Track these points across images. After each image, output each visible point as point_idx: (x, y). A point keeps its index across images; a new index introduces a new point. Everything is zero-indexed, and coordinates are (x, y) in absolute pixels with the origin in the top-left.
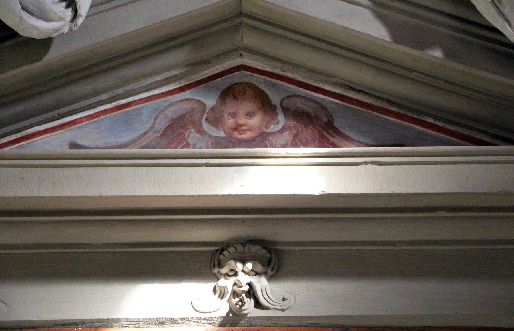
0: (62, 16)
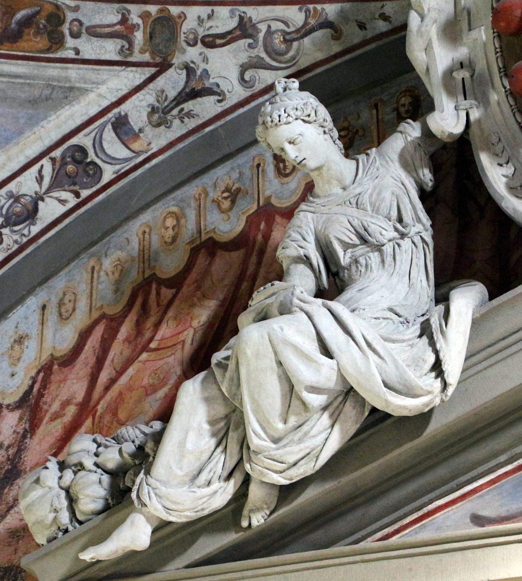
0: (429, 389)
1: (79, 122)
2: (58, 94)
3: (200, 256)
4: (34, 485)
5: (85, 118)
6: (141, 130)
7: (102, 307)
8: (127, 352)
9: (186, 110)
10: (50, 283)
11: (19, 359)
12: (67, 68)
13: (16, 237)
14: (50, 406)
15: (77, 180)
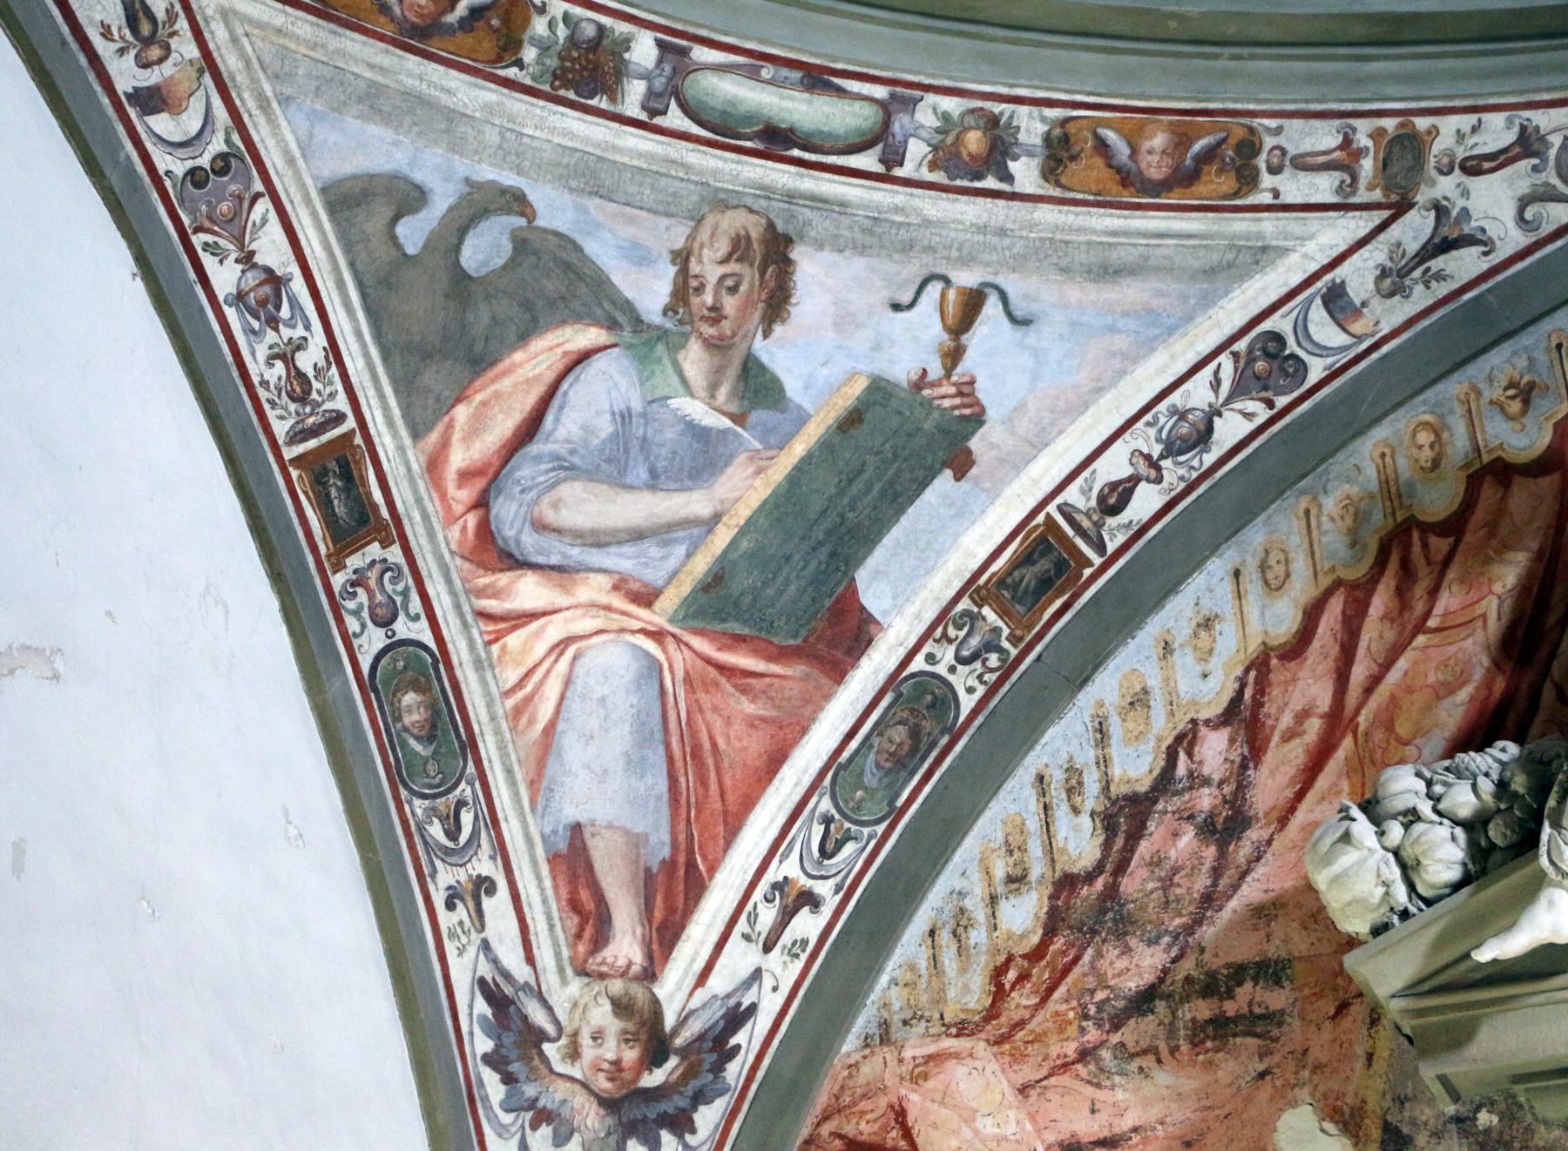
1: (1274, 297)
2: (1245, 258)
3: (1486, 486)
4: (1340, 845)
5: (1284, 291)
6: (1364, 304)
7: (1333, 569)
8: (1390, 635)
9: (1434, 270)
10: (1240, 536)
11: (1211, 651)
12: (1259, 220)
13: (1182, 471)
14: (1277, 719)
15: (1271, 382)
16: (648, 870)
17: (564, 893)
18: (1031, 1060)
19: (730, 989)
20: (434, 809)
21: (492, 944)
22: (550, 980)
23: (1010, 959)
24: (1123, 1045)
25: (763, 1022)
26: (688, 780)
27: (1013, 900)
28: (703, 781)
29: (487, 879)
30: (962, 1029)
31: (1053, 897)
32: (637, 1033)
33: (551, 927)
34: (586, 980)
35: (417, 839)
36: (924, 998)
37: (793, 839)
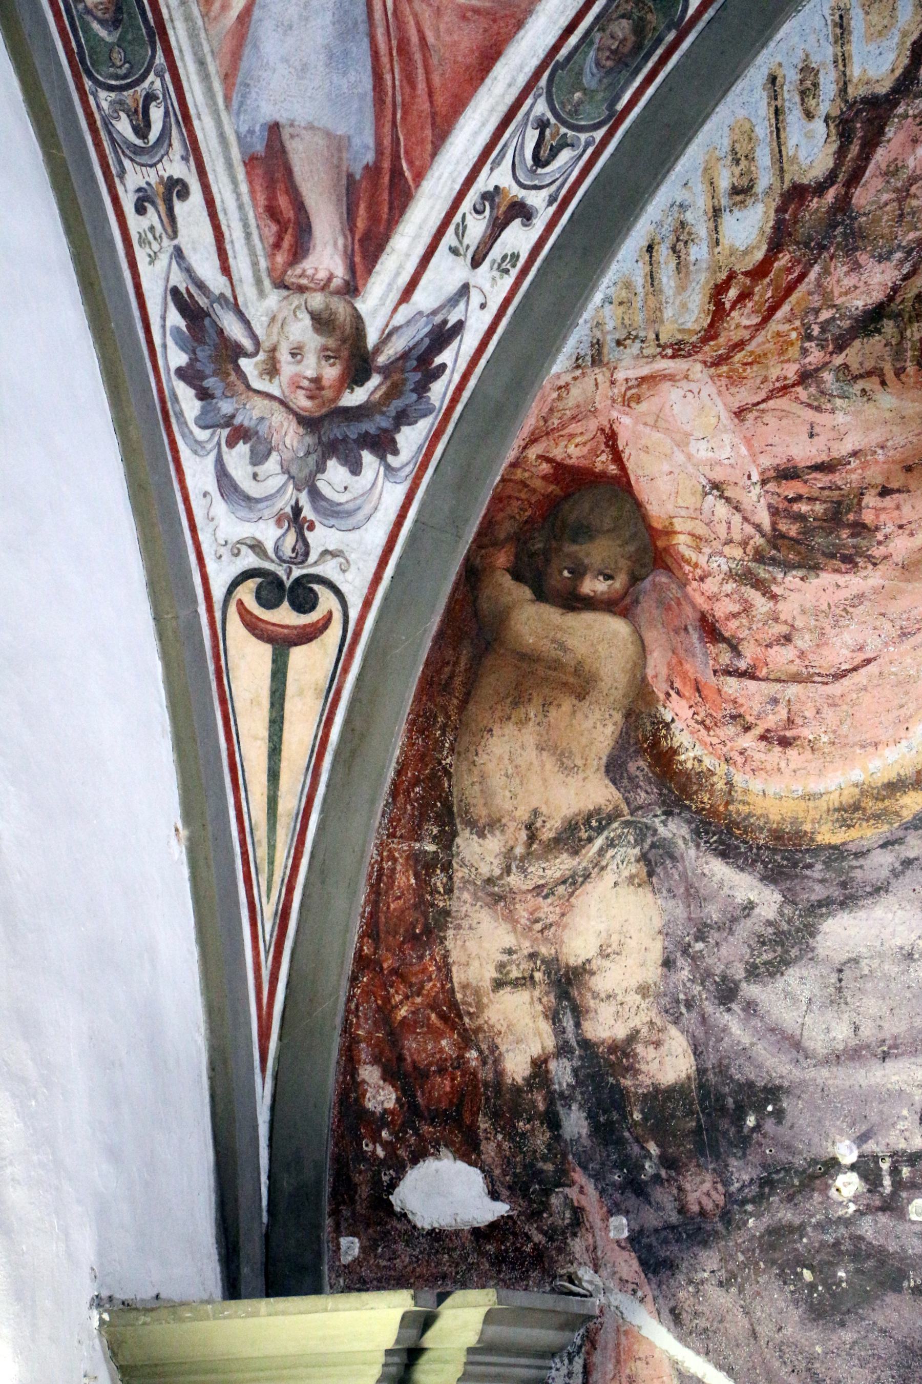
16: (350, 176)
17: (262, 200)
18: (749, 383)
19: (436, 305)
20: (121, 103)
21: (186, 252)
22: (247, 292)
23: (731, 276)
24: (846, 366)
25: (469, 341)
26: (393, 78)
27: (737, 213)
28: (410, 79)
29: (180, 181)
30: (678, 350)
31: (780, 210)
32: (337, 350)
33: (248, 236)
34: (285, 293)
35: (103, 134)
36: (639, 318)
37: (505, 145)
